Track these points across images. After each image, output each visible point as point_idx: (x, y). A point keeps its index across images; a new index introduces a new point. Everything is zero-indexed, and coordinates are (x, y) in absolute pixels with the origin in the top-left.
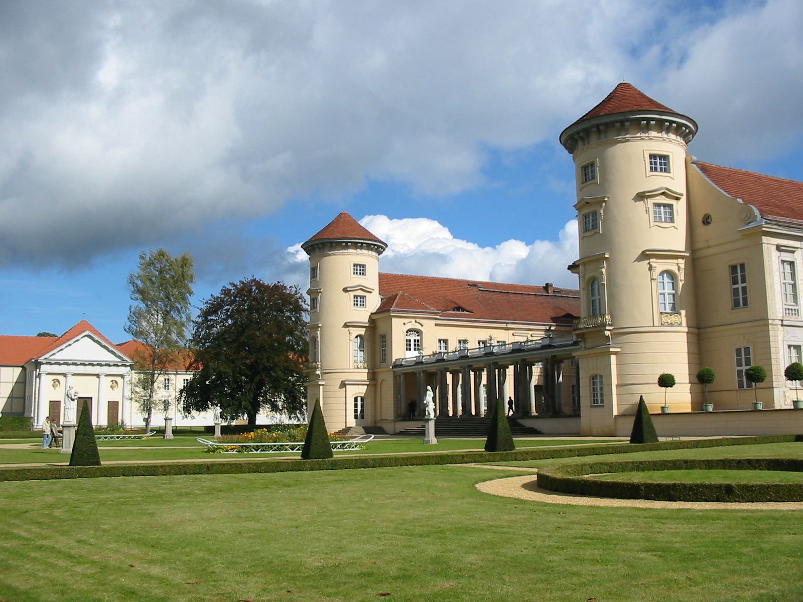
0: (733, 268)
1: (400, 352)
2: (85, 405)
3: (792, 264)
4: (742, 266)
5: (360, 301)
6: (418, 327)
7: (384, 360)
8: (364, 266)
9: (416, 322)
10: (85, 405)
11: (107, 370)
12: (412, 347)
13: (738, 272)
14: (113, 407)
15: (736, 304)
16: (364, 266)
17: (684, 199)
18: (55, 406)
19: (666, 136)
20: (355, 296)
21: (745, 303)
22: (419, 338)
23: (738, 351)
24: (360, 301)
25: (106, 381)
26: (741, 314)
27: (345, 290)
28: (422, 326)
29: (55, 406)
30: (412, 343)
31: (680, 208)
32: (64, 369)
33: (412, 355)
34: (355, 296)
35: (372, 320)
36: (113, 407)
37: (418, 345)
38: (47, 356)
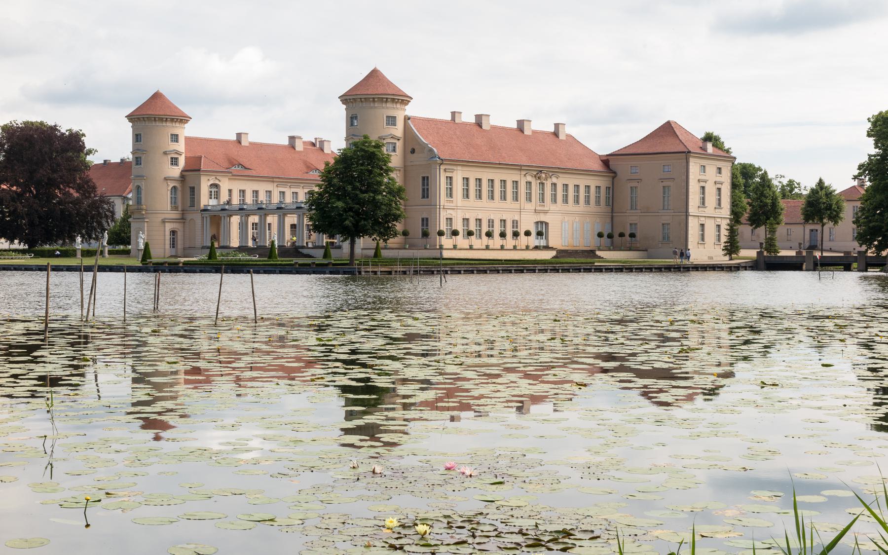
0: (424, 178)
1: (205, 200)
3: (451, 178)
4: (428, 177)
6: (217, 182)
7: (193, 205)
8: (177, 135)
9: (216, 178)
12: (213, 196)
13: (425, 180)
15: (423, 197)
16: (177, 135)
17: (401, 141)
19: (395, 106)
20: (172, 158)
21: (428, 197)
22: (216, 190)
23: (423, 219)
24: (174, 162)
27: (165, 153)
28: (220, 181)
30: (213, 193)
31: (399, 145)
33: (213, 202)
34: (172, 158)
35: (183, 177)
37: (217, 196)
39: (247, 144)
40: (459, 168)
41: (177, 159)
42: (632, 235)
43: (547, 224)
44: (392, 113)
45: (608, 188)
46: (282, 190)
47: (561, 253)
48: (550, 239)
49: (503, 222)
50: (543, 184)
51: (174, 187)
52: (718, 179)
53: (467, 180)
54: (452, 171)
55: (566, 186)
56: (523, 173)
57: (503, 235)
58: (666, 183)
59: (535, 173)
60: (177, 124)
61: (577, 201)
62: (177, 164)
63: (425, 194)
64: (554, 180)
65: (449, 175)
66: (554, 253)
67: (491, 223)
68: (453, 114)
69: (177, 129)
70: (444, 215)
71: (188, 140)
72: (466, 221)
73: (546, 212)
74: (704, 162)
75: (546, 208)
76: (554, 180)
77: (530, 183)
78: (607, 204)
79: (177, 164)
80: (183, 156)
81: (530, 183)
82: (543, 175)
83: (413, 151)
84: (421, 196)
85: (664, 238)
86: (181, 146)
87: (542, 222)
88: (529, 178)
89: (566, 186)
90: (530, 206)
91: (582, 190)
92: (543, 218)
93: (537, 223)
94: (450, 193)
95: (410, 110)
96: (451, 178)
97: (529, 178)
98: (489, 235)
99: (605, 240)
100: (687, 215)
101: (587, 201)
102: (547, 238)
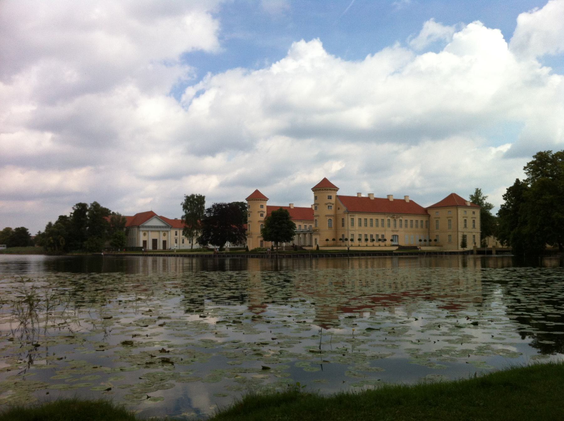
2: (155, 242)
3: (353, 219)
5: (262, 215)
8: (263, 205)
10: (155, 242)
11: (162, 229)
14: (164, 242)
16: (263, 205)
17: (334, 205)
18: (145, 242)
25: (162, 234)
26: (343, 228)
29: (145, 242)
31: (333, 207)
32: (148, 229)
34: (261, 214)
36: (164, 242)
38: (142, 225)
39: (293, 208)
40: (357, 215)
41: (263, 214)
42: (436, 240)
43: (398, 236)
44: (330, 195)
45: (426, 221)
46: (305, 224)
47: (401, 248)
48: (399, 241)
49: (366, 235)
50: (396, 220)
51: (262, 225)
52: (473, 216)
53: (360, 219)
54: (354, 216)
55: (406, 221)
56: (386, 216)
57: (359, 240)
58: (450, 219)
59: (392, 216)
60: (263, 201)
61: (412, 226)
62: (263, 216)
63: (343, 225)
64: (401, 218)
65: (352, 217)
66: (397, 248)
67: (372, 236)
68: (358, 193)
69: (262, 203)
70: (350, 233)
71: (268, 207)
72: (366, 235)
73: (397, 231)
74: (465, 209)
75: (397, 229)
76: (401, 218)
77: (389, 220)
78: (427, 227)
79: (263, 216)
80: (266, 213)
81: (389, 220)
82: (395, 217)
83: (339, 209)
84: (341, 226)
85: (449, 241)
86: (265, 209)
87: (395, 235)
88: (389, 218)
89: (406, 221)
90: (390, 229)
91: (419, 222)
92: (395, 233)
93: (393, 235)
94: (353, 224)
95: (339, 193)
96: (353, 219)
97: (389, 218)
98: (352, 240)
99: (423, 242)
100: (458, 232)
101: (417, 226)
102: (398, 241)
